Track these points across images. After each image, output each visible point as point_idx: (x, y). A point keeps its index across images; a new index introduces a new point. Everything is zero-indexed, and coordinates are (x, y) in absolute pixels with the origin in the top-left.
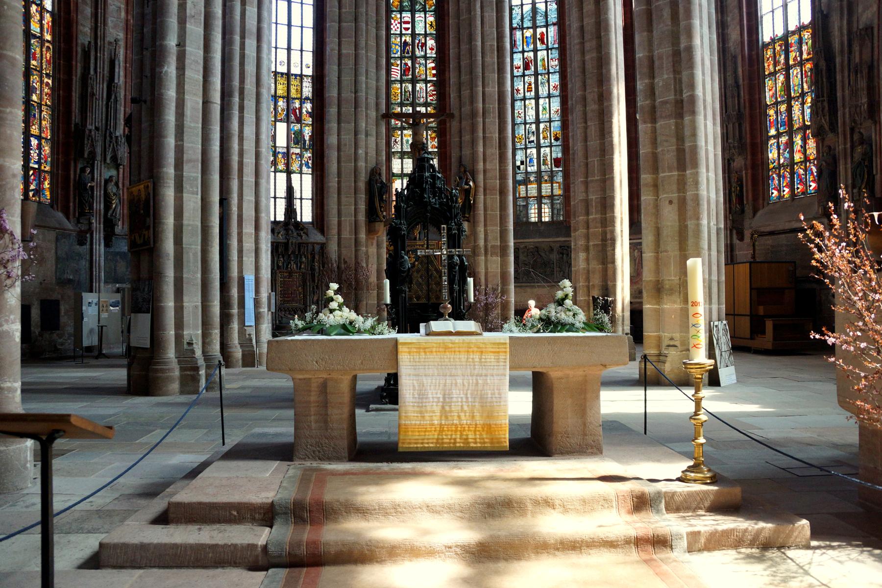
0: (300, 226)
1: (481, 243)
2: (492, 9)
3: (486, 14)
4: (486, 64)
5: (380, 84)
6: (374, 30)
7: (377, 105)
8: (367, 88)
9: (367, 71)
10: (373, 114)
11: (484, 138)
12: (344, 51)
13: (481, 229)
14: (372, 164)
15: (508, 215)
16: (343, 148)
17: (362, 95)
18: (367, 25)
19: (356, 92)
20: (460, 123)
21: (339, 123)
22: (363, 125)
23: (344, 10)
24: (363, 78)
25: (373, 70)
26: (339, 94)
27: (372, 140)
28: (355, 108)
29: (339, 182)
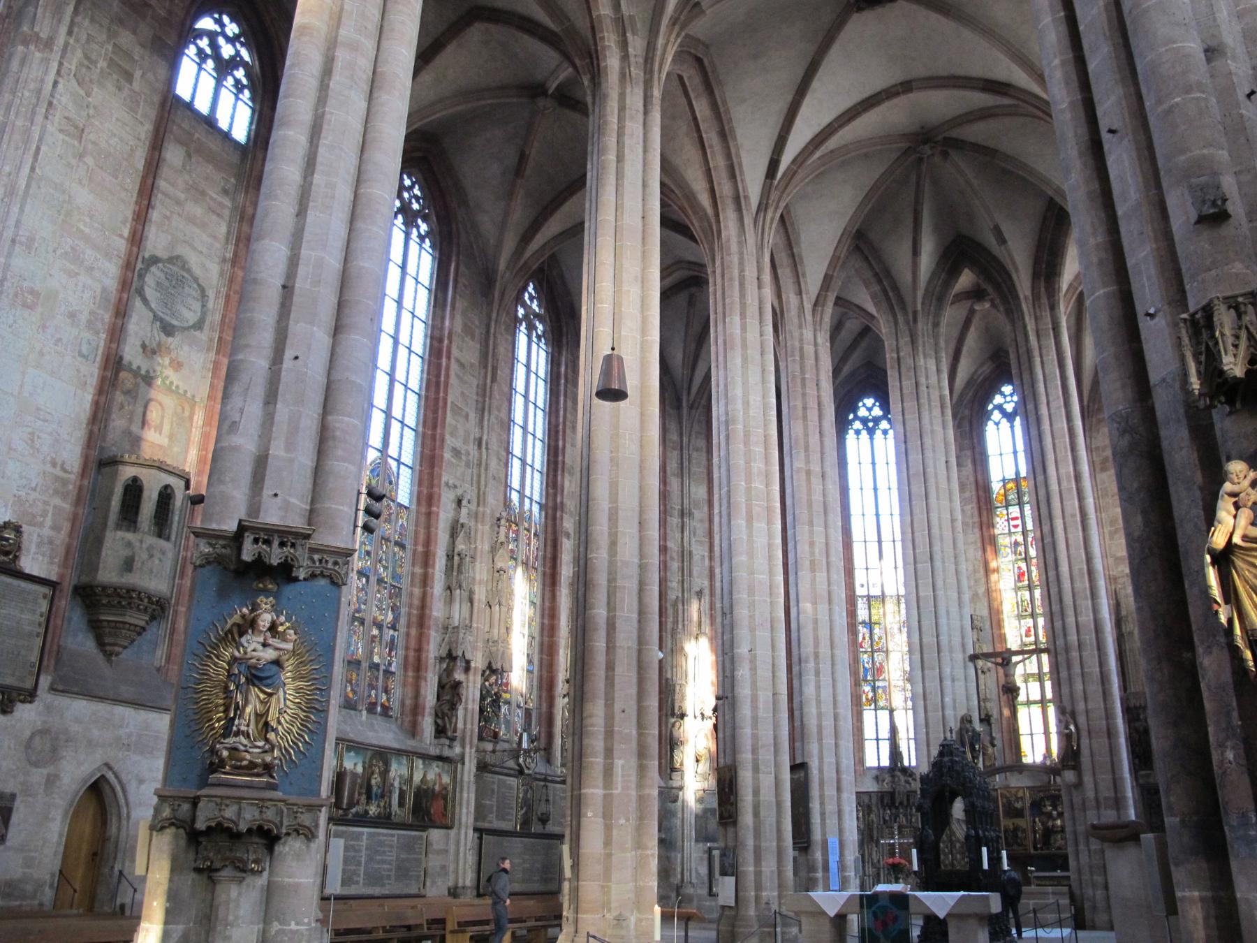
0: (905, 770)
1: (1091, 794)
2: (1077, 529)
3: (1070, 536)
4: (1076, 590)
5: (964, 622)
6: (953, 567)
7: (963, 646)
8: (949, 629)
9: (948, 612)
10: (959, 656)
11: (1082, 674)
12: (921, 594)
13: (1088, 779)
14: (962, 712)
15: (1120, 761)
16: (928, 697)
17: (944, 639)
18: (943, 562)
19: (938, 636)
20: (1056, 657)
21: (923, 670)
22: (947, 670)
23: (917, 551)
24: (943, 621)
25: (954, 609)
26: (921, 639)
27: (960, 685)
28: (939, 653)
29: (927, 733)
